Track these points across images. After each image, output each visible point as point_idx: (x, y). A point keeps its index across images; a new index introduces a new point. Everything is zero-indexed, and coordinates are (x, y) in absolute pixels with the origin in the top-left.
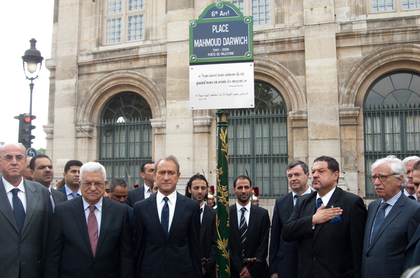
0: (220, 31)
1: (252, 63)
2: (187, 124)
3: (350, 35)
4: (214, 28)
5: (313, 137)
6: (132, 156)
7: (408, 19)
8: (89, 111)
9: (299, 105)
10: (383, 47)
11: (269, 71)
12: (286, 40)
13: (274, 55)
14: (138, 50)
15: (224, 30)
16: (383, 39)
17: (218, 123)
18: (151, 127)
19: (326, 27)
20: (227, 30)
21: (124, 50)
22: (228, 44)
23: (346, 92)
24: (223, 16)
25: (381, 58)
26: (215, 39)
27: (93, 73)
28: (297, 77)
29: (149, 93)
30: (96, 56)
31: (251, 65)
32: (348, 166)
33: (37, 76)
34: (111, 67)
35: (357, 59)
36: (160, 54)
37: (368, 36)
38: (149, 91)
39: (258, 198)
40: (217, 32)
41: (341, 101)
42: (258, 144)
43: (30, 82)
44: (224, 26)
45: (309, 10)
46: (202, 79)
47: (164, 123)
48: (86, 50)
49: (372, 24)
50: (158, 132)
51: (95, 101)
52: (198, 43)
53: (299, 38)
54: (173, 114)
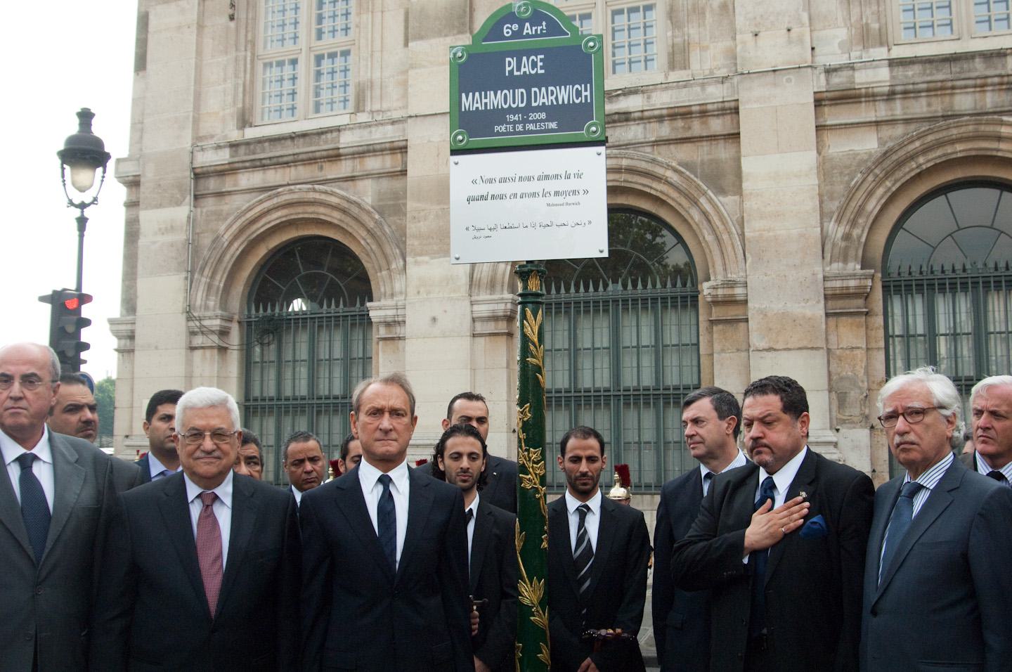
0: (525, 72)
1: (602, 149)
2: (457, 314)
3: (848, 97)
4: (509, 65)
5: (763, 345)
6: (323, 389)
8: (220, 281)
9: (728, 266)
10: (928, 123)
11: (655, 185)
12: (694, 109)
13: (666, 146)
14: (339, 137)
15: (533, 69)
16: (929, 105)
17: (520, 295)
18: (370, 323)
19: (791, 77)
20: (541, 68)
21: (304, 135)
22: (544, 103)
23: (840, 235)
24: (532, 36)
25: (925, 151)
26: (511, 91)
27: (230, 193)
28: (721, 198)
29: (364, 239)
30: (236, 151)
31: (599, 154)
32: (847, 414)
33: (95, 199)
34: (273, 177)
35: (866, 153)
36: (392, 145)
37: (892, 99)
38: (364, 234)
39: (628, 491)
40: (516, 73)
41: (828, 256)
42: (628, 362)
43: (77, 212)
44: (533, 60)
45: (749, 37)
46: (482, 189)
47: (400, 312)
48: (212, 137)
49: (901, 69)
50: (386, 333)
51: (234, 259)
52: (471, 102)
53: (727, 105)
54: (422, 290)
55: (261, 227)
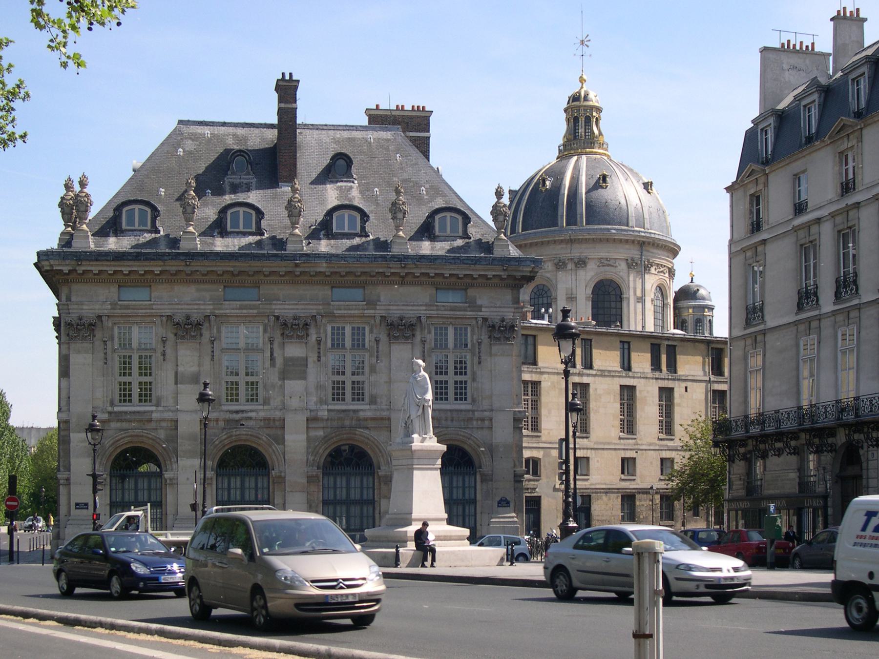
3: (315, 419)
7: (355, 411)
21: (138, 412)
34: (125, 425)
55: (120, 443)
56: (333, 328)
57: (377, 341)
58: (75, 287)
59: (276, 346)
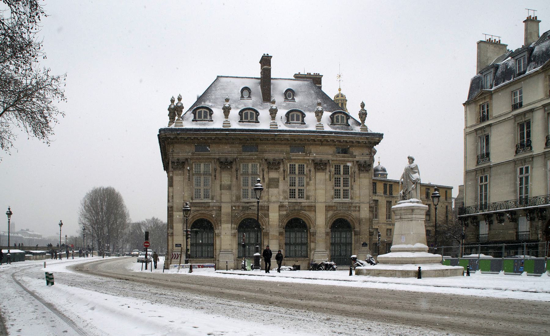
7: (300, 203)
42: (251, 239)
56: (290, 165)
57: (310, 171)
58: (176, 145)
59: (265, 173)
